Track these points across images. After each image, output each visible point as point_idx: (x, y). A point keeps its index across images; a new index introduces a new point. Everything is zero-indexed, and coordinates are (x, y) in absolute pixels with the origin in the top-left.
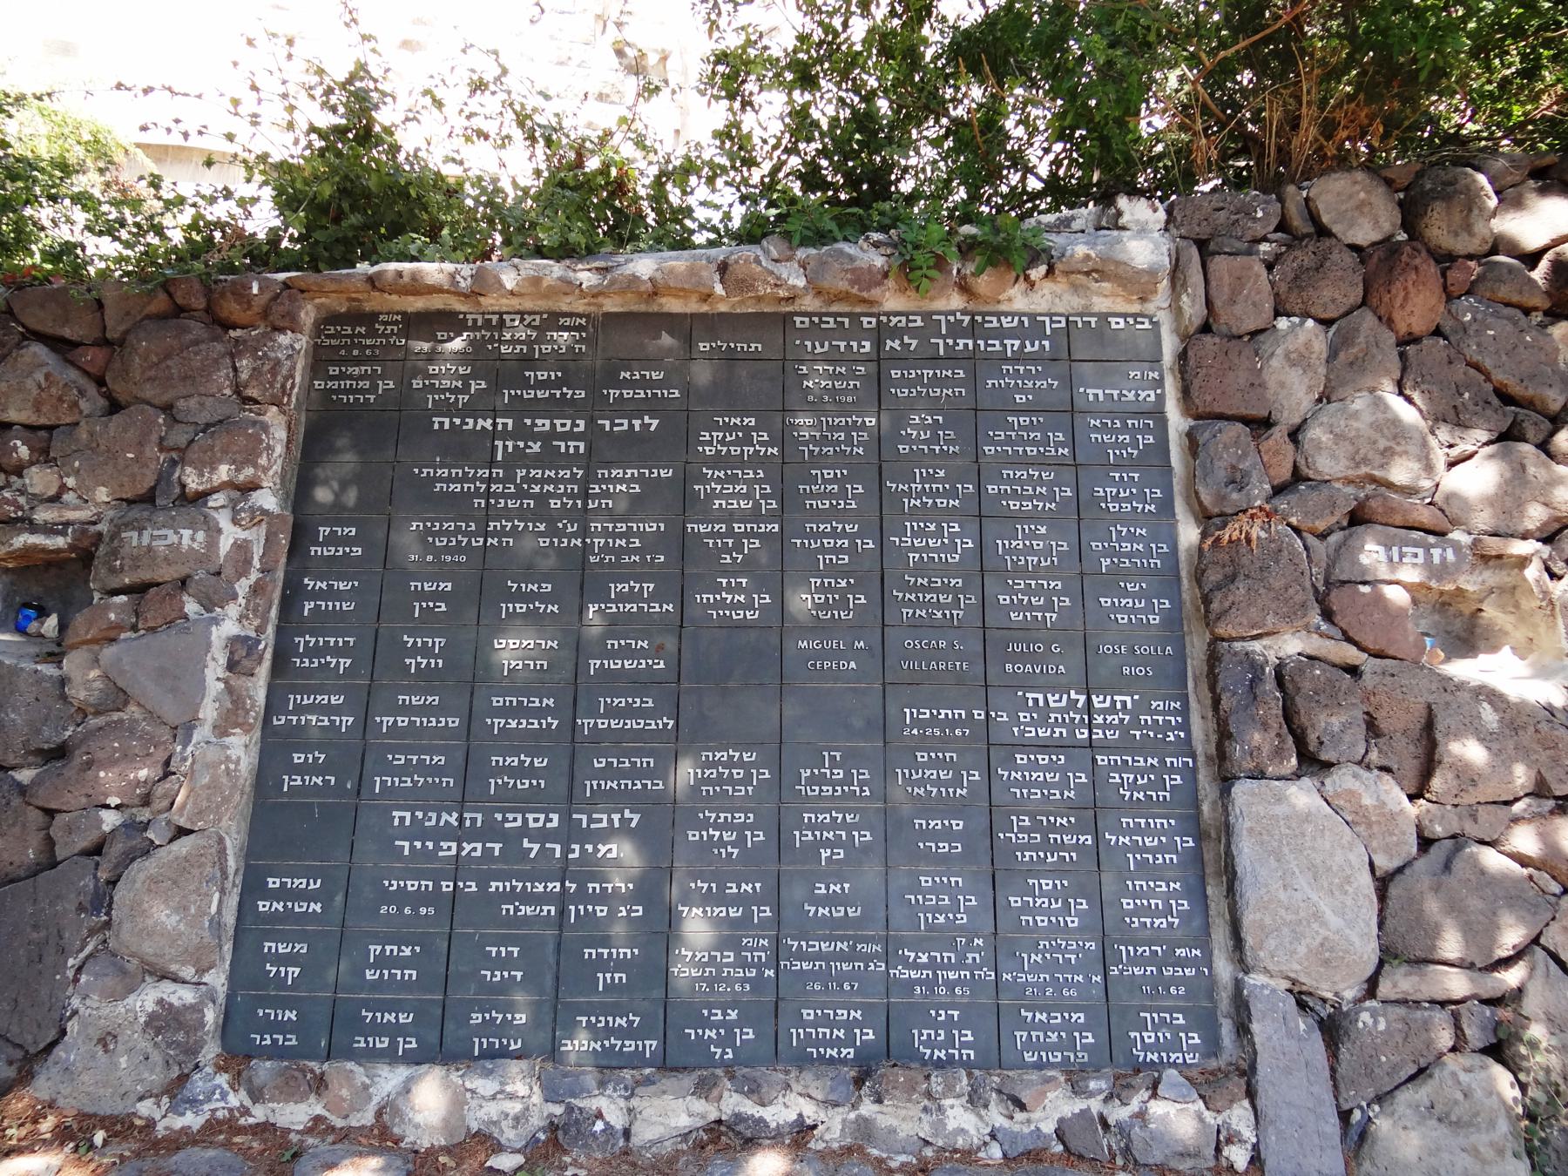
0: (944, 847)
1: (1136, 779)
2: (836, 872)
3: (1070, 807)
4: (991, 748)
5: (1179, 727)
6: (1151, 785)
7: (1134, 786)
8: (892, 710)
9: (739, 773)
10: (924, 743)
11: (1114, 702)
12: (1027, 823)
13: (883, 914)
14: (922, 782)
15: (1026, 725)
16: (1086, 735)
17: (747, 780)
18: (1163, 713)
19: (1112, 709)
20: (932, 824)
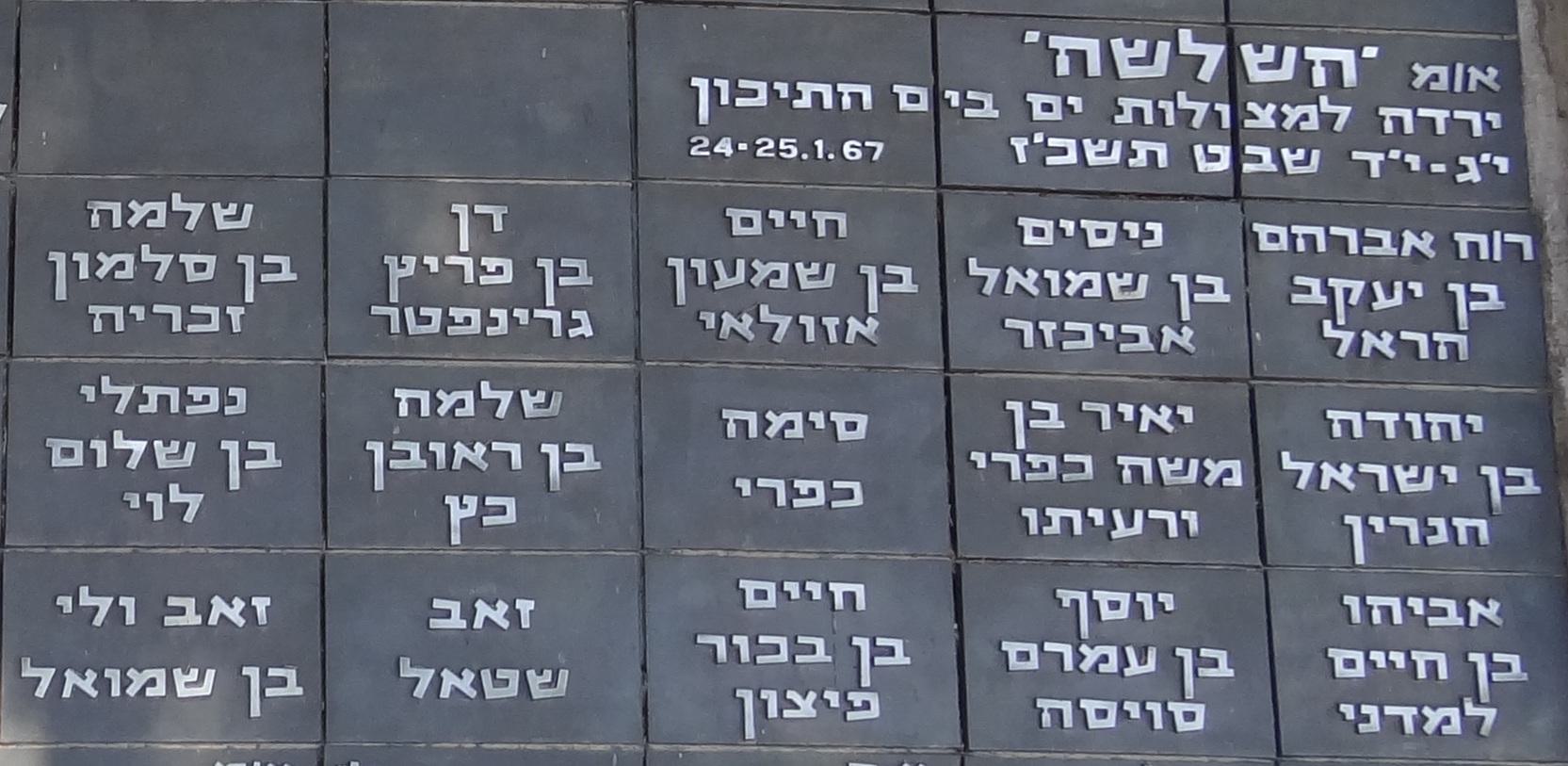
0: (812, 493)
1: (1369, 294)
2: (490, 565)
3: (1174, 377)
4: (949, 197)
5: (1494, 142)
6: (1412, 313)
7: (1363, 316)
8: (655, 82)
9: (200, 266)
10: (750, 180)
11: (1305, 67)
12: (1055, 423)
13: (629, 692)
14: (746, 299)
15: (1051, 129)
16: (1224, 164)
17: (226, 288)
18: (1448, 100)
19: (1301, 89)
20: (777, 421)
